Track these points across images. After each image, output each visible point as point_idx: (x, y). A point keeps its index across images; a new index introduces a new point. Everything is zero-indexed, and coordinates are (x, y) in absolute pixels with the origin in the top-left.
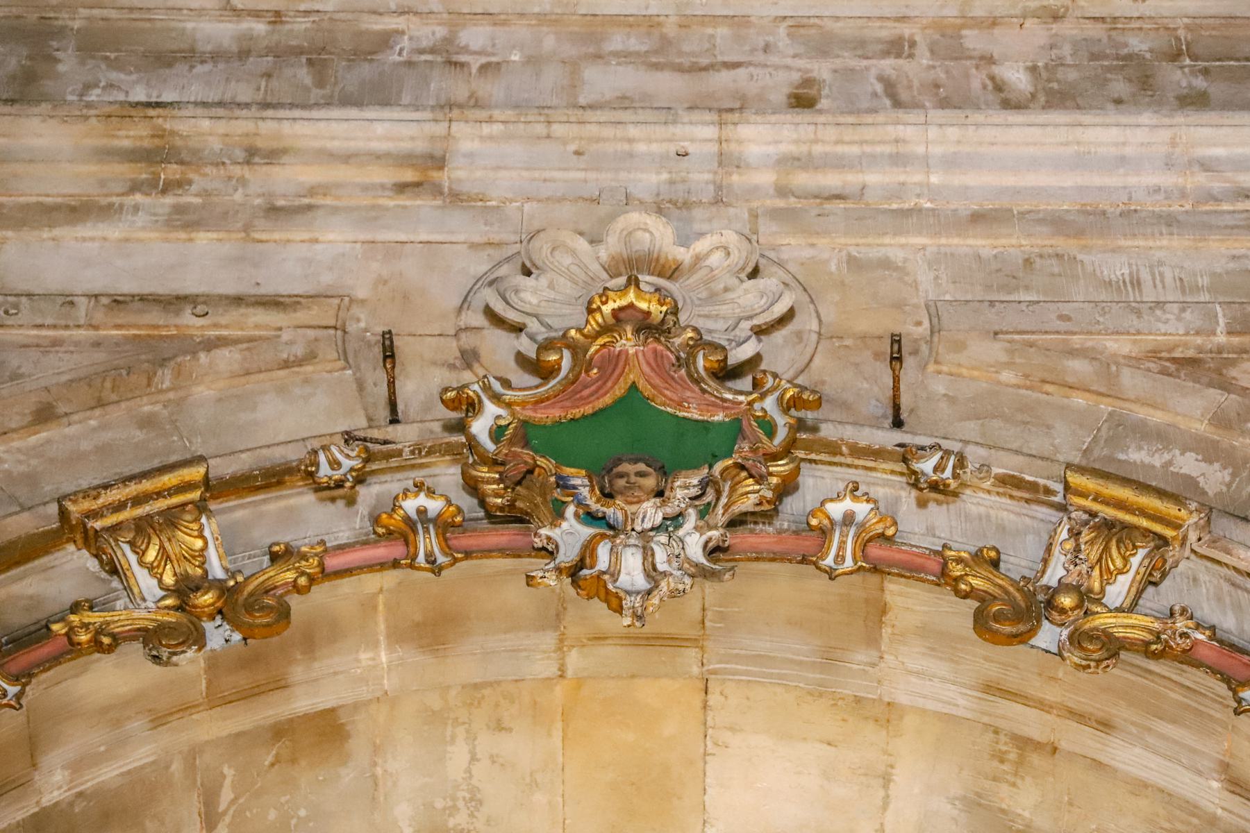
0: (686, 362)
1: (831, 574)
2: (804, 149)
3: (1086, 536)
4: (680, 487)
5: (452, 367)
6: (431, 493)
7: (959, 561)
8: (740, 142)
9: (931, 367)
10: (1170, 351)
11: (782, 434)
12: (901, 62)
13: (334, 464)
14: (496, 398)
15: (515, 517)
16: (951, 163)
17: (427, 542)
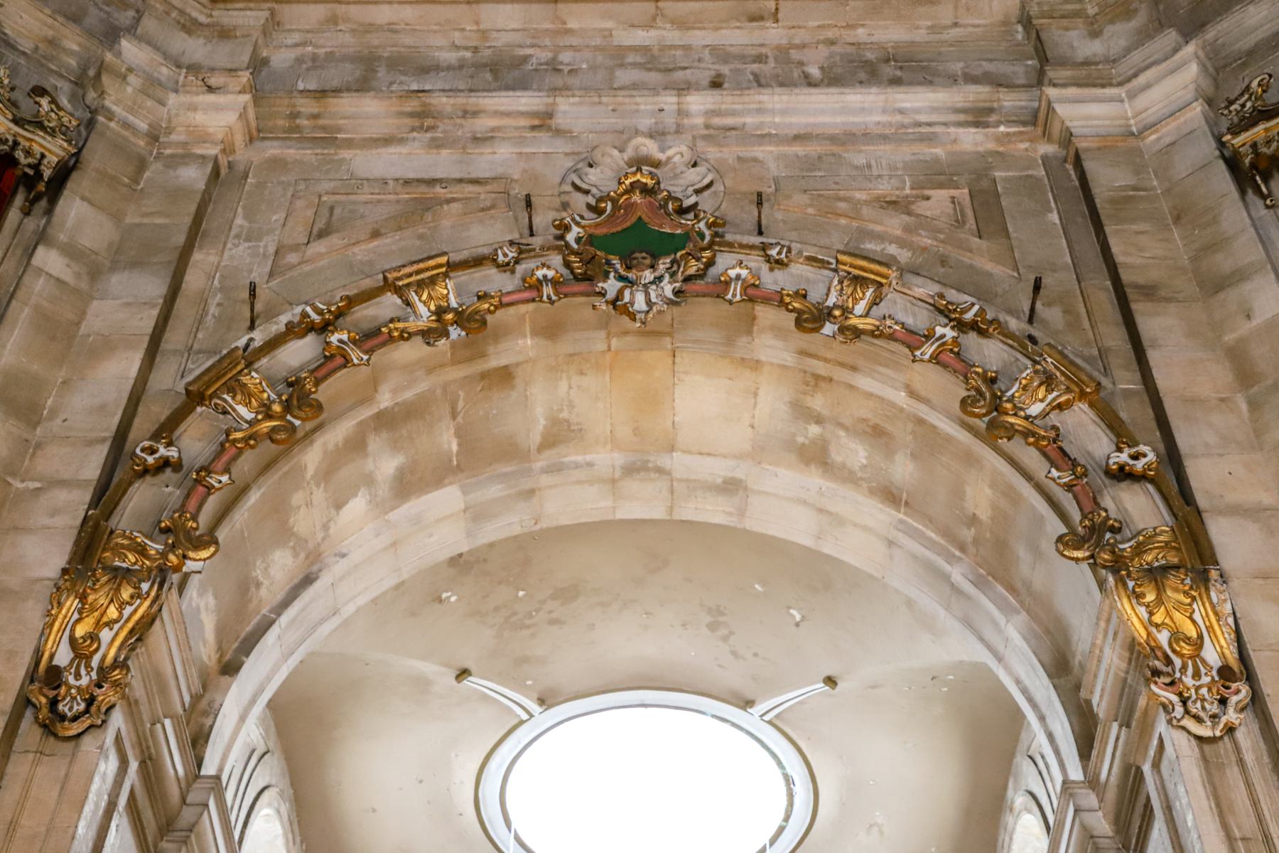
0: (665, 207)
1: (730, 302)
2: (717, 107)
3: (846, 283)
5: (557, 210)
6: (549, 267)
7: (788, 295)
8: (688, 104)
9: (776, 207)
10: (885, 197)
11: (707, 239)
12: (761, 65)
13: (505, 255)
14: (578, 224)
15: (587, 278)
16: (784, 112)
17: (547, 290)
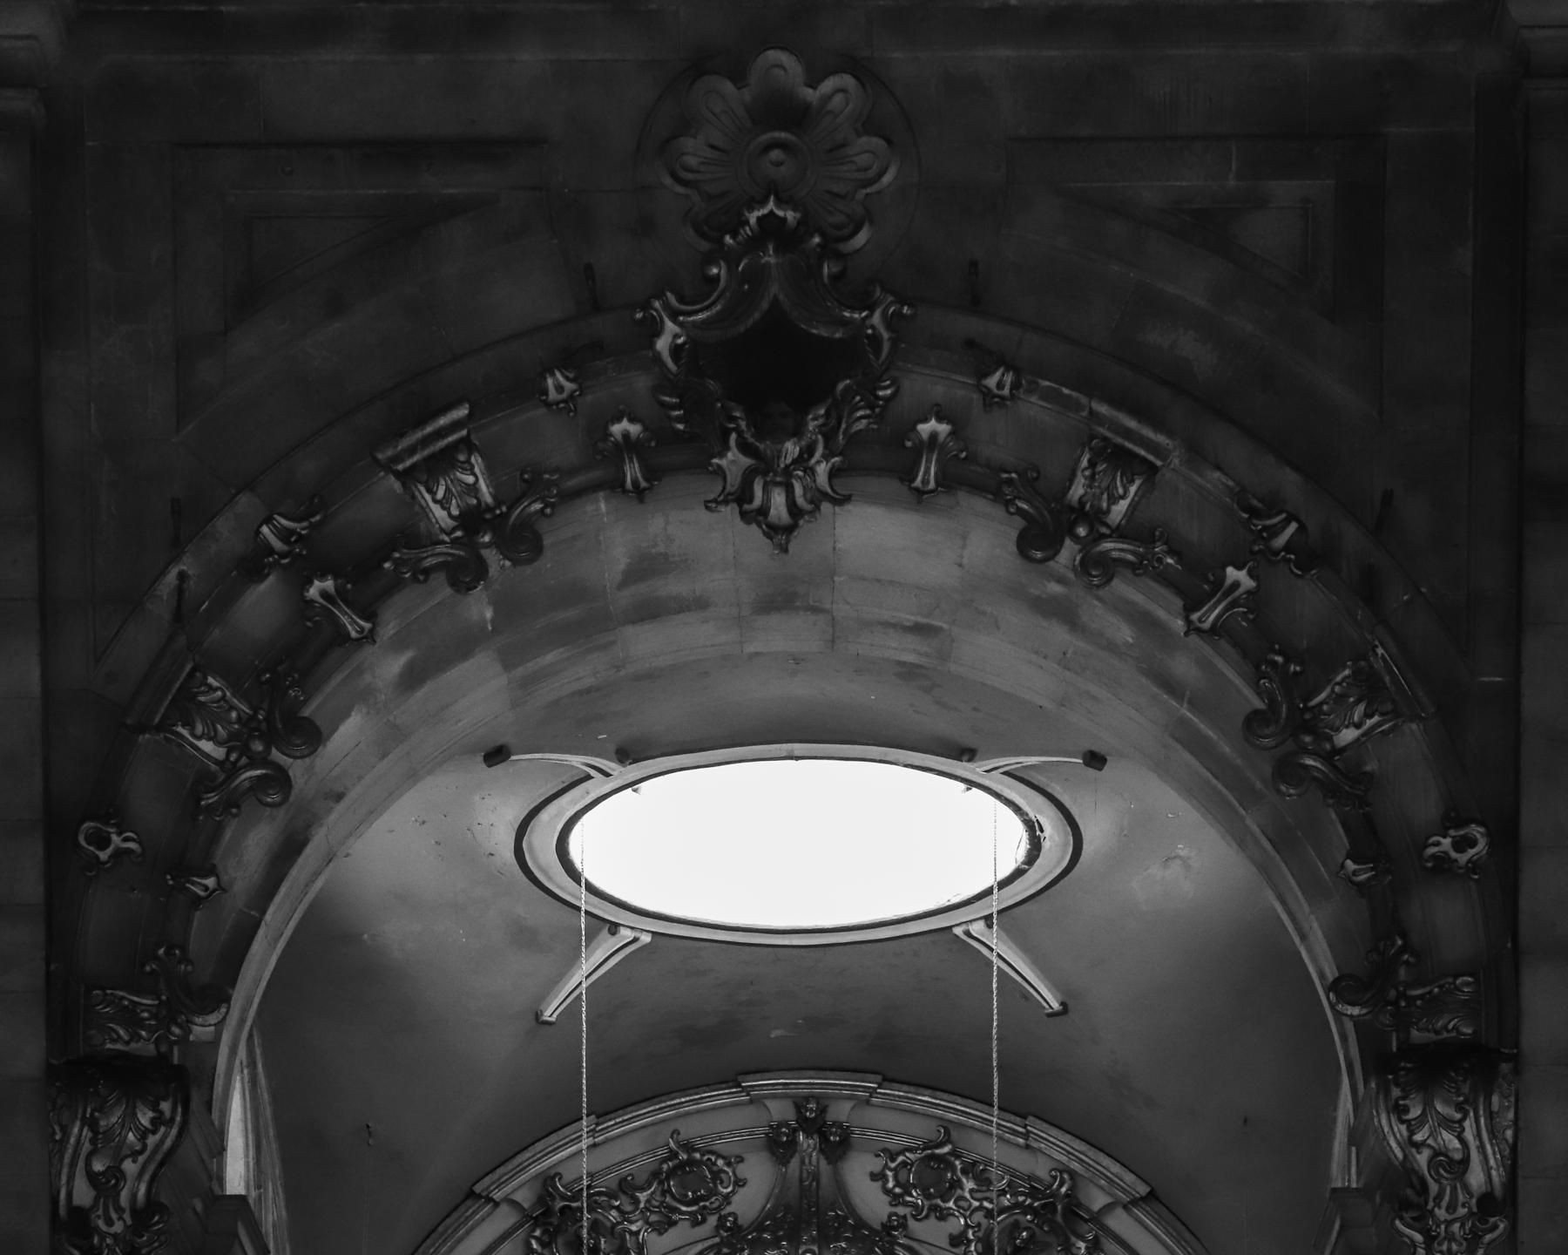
3: (1100, 468)
4: (812, 419)
7: (1010, 482)
13: (560, 389)
14: (674, 315)
